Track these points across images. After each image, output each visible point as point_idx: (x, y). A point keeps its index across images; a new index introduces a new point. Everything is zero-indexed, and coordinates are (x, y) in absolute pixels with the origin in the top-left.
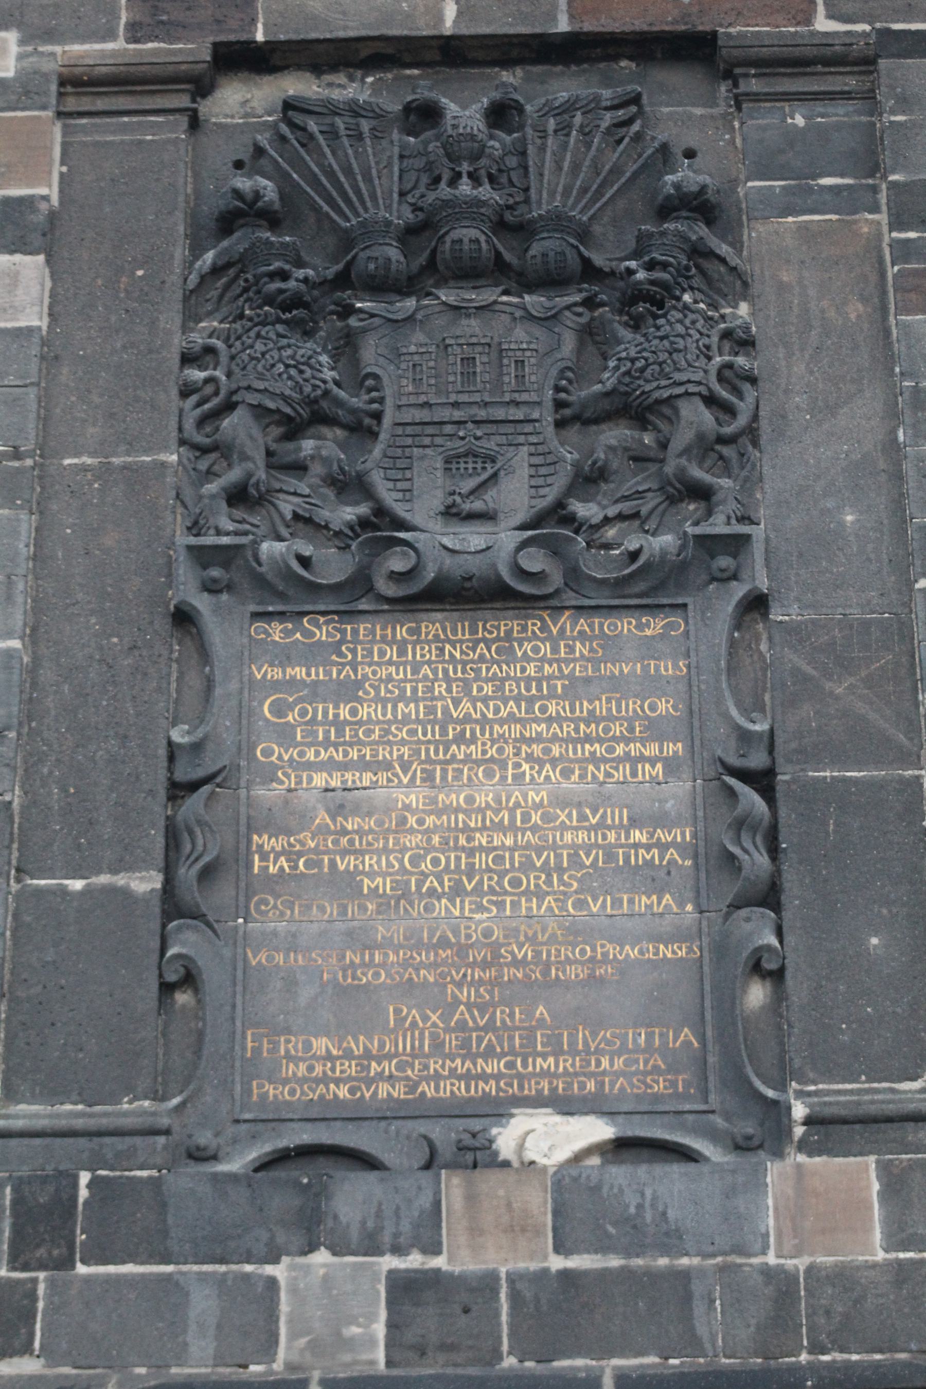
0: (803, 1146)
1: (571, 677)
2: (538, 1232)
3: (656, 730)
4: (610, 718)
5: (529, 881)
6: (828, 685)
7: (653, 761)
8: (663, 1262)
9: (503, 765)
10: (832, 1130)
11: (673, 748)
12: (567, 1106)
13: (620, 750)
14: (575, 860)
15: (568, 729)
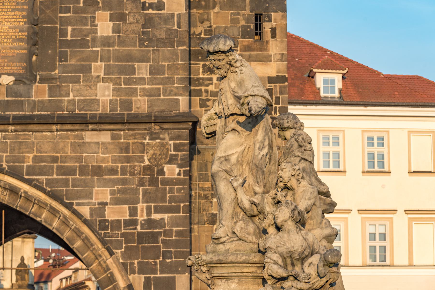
0: (38, 83)
1: (12, 8)
2: (4, 95)
3: (23, 17)
4: (17, 15)
5: (5, 40)
6: (46, 11)
7: (22, 22)
8: (20, 99)
9: (2, 22)
10: (43, 80)
11: (25, 20)
12: (9, 74)
13: (18, 20)
14: (11, 38)
15: (11, 17)
